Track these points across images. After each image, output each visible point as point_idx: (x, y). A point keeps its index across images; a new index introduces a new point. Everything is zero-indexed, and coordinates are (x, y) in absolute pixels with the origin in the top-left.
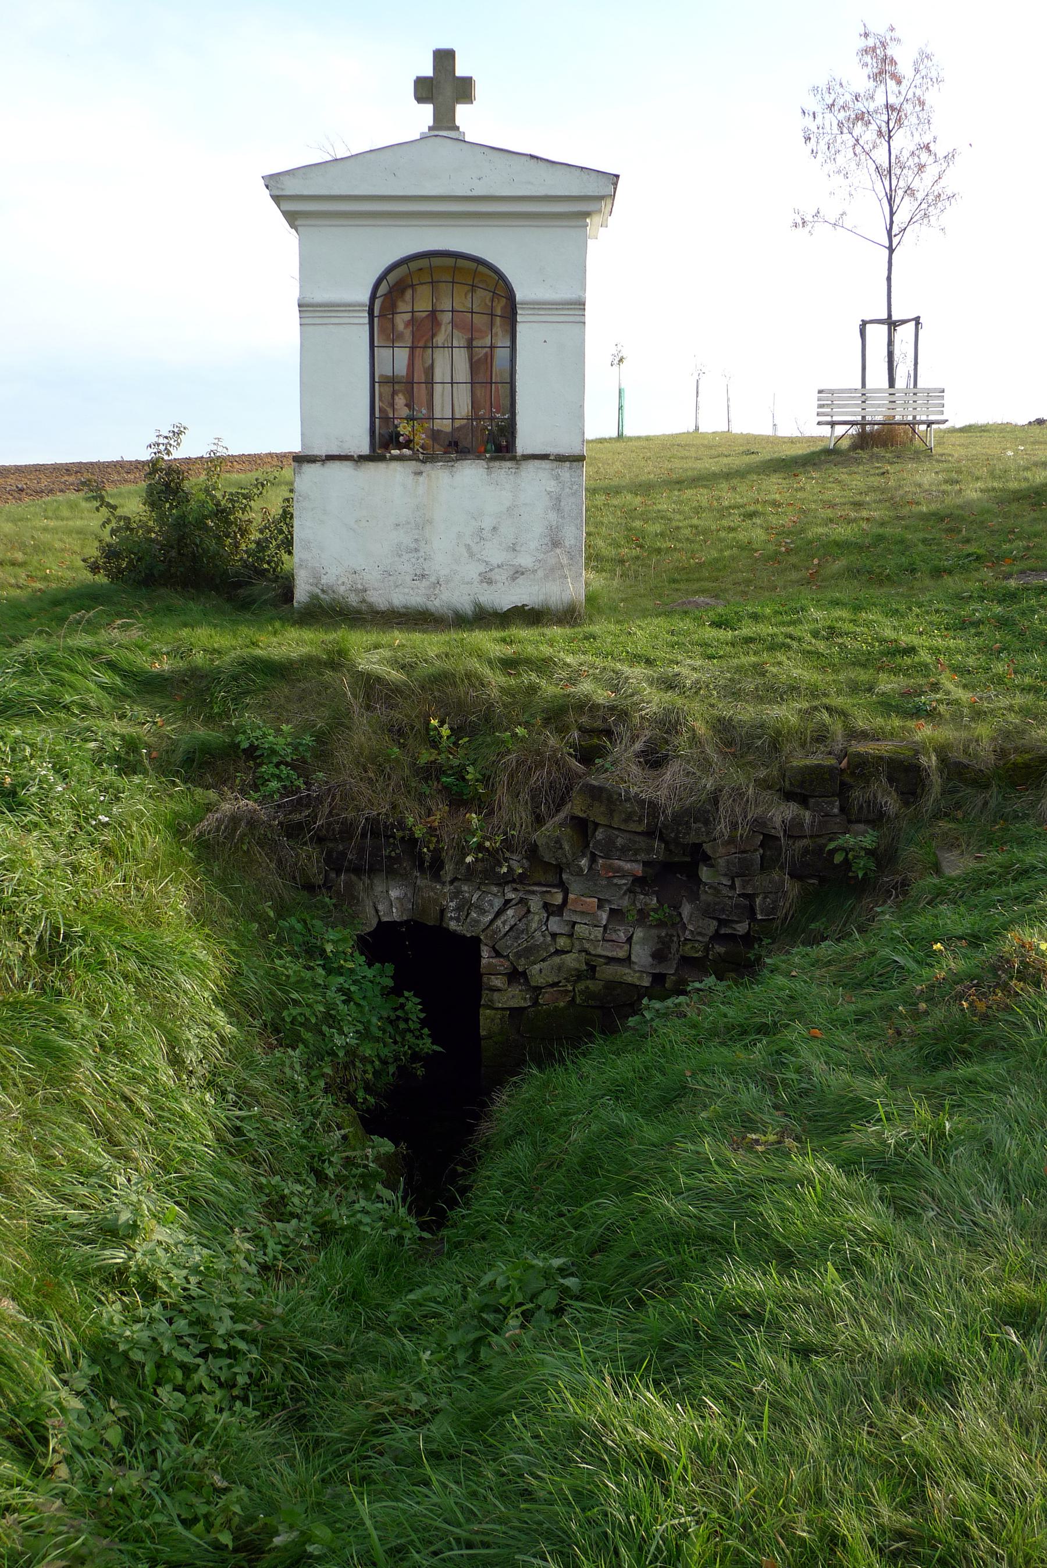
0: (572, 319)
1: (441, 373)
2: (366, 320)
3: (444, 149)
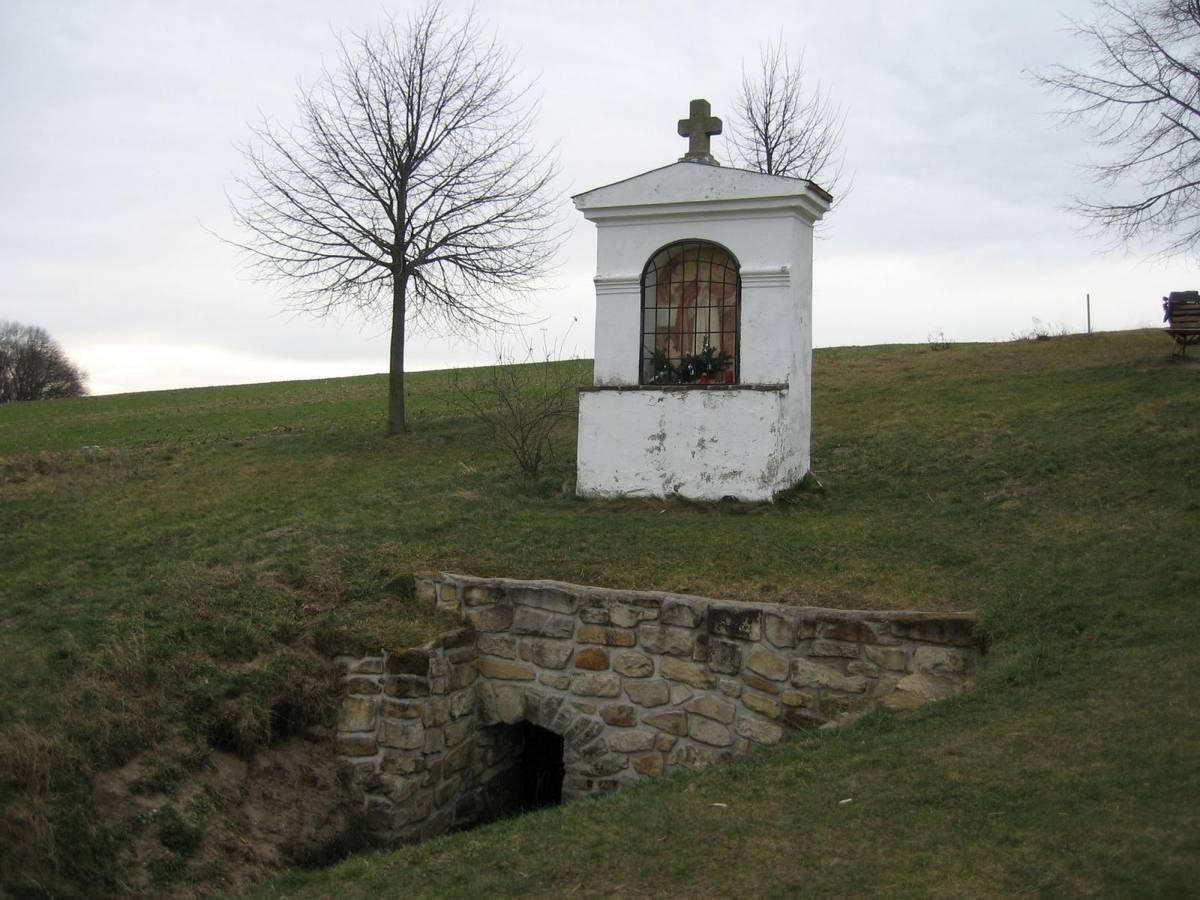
0: (777, 284)
1: (701, 326)
2: (639, 290)
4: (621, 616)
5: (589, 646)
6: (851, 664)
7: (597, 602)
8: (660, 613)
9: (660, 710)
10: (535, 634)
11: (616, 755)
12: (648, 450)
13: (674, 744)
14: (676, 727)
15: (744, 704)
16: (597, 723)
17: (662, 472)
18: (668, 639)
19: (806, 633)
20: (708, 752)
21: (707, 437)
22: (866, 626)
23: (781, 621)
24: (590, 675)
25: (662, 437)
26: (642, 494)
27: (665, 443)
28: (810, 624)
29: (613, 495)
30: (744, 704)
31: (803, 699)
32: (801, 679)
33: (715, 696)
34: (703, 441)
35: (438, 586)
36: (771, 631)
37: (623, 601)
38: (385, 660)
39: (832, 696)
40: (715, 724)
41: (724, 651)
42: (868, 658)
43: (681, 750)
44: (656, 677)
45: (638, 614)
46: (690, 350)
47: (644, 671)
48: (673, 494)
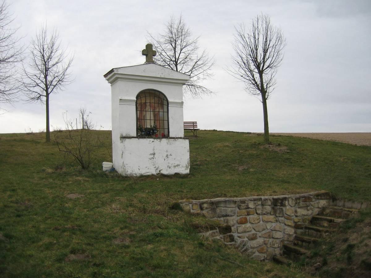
1: (148, 117)
2: (135, 104)
3: (151, 66)
4: (251, 205)
5: (241, 217)
6: (309, 208)
7: (243, 202)
8: (262, 203)
9: (264, 232)
10: (227, 216)
11: (252, 249)
12: (149, 159)
13: (268, 241)
14: (269, 236)
15: (285, 224)
16: (247, 241)
17: (155, 166)
18: (264, 210)
19: (298, 201)
20: (278, 241)
21: (169, 154)
22: (310, 197)
23: (292, 199)
24: (243, 226)
25: (154, 154)
26: (149, 174)
27: (155, 156)
28: (299, 199)
29: (138, 175)
30: (285, 224)
31: (299, 219)
32: (298, 214)
33: (278, 224)
34: (167, 155)
35: (191, 205)
36: (290, 202)
37: (251, 200)
38: (218, 230)
39: (305, 217)
40: (279, 232)
41: (280, 210)
42: (311, 205)
43: (271, 242)
44: (261, 222)
45: (256, 203)
46: (145, 126)
47: (258, 221)
48: (159, 173)
